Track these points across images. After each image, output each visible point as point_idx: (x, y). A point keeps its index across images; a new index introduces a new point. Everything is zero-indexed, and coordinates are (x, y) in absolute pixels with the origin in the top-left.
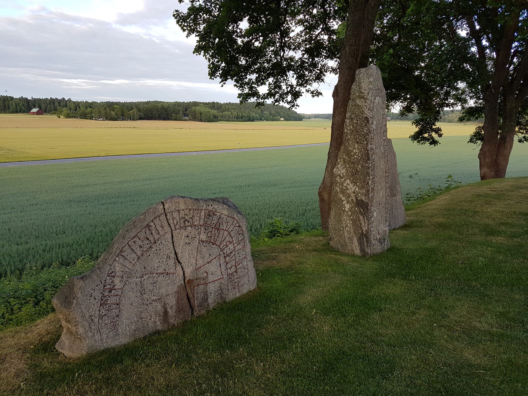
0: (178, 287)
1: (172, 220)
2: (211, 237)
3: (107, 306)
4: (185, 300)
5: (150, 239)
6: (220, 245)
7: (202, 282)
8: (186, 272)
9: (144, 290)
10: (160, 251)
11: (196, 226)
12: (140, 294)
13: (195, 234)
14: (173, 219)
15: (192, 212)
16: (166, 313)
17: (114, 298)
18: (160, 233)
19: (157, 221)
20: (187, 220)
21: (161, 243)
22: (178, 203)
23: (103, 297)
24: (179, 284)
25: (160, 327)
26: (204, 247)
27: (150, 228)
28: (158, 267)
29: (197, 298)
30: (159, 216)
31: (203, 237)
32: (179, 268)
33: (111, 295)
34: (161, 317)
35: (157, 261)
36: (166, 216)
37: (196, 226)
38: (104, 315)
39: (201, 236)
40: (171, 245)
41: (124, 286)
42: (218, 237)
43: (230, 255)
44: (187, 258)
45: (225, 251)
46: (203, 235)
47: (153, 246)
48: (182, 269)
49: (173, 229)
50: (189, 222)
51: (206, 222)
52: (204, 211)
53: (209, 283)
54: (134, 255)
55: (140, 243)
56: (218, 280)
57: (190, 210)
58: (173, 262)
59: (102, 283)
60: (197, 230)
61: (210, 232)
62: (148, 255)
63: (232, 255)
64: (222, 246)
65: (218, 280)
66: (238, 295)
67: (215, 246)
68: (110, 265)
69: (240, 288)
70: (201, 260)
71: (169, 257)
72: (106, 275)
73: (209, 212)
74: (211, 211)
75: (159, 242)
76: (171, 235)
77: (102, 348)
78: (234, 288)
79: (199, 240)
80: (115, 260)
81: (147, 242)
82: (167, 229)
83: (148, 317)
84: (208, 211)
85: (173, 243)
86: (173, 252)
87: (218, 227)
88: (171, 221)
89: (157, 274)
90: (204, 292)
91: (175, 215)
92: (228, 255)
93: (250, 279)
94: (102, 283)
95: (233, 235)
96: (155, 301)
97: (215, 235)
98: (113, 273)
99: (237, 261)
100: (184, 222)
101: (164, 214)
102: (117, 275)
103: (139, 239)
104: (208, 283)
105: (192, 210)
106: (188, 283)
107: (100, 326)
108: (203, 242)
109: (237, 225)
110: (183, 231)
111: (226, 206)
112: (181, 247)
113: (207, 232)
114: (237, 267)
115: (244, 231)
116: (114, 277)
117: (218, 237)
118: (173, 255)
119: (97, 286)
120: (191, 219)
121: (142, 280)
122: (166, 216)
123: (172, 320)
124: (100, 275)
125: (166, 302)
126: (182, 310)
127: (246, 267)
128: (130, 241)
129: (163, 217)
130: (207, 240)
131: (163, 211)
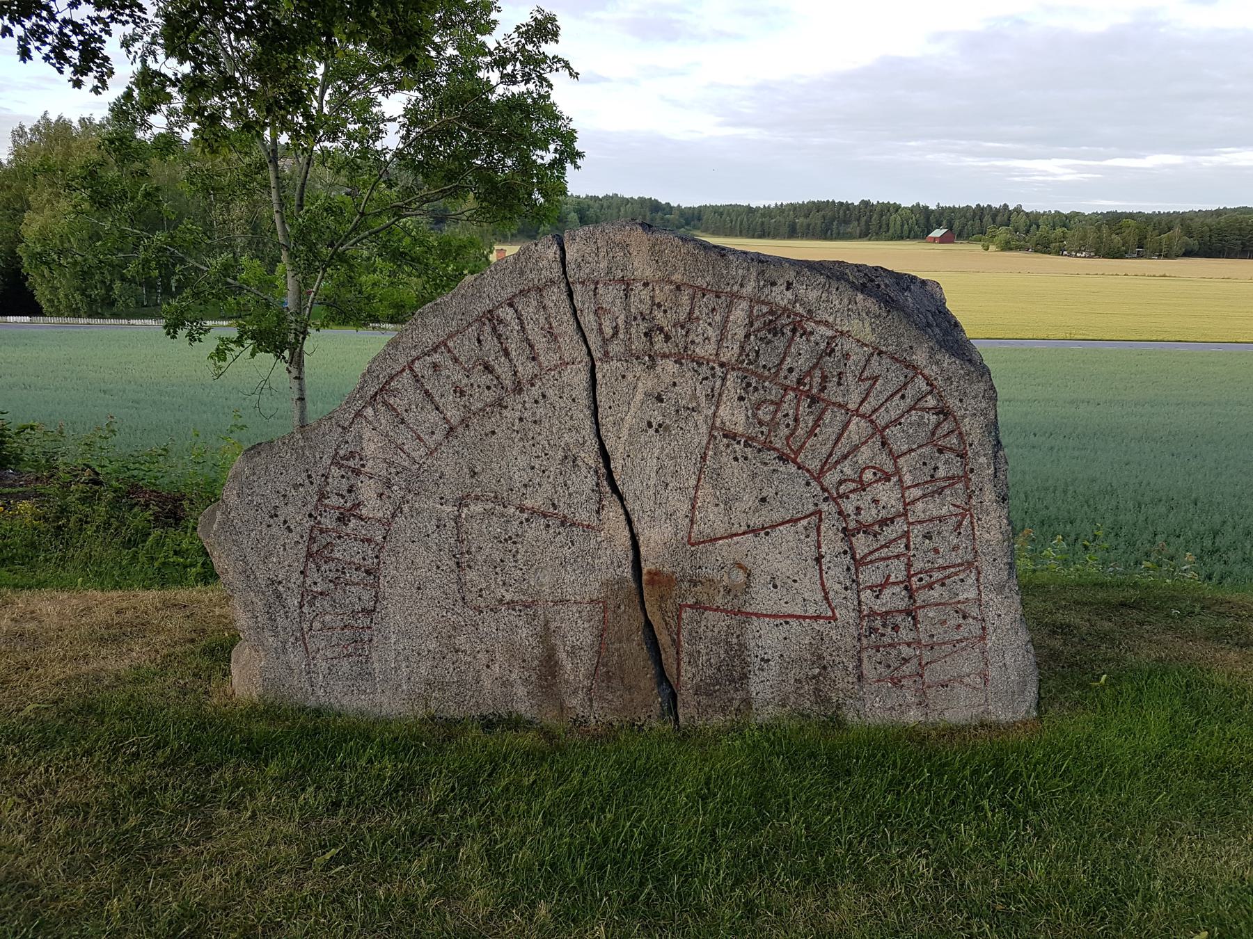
0: (606, 584)
1: (592, 317)
2: (773, 425)
3: (332, 565)
4: (635, 647)
5: (498, 370)
6: (822, 471)
7: (719, 601)
8: (642, 538)
9: (469, 552)
10: (537, 428)
11: (700, 364)
12: (452, 564)
13: (694, 396)
14: (599, 311)
15: (685, 299)
16: (549, 666)
17: (356, 546)
18: (541, 358)
19: (529, 309)
20: (661, 329)
21: (544, 396)
22: (625, 247)
23: (316, 532)
24: (609, 574)
25: (524, 707)
26: (736, 459)
27: (501, 328)
28: (525, 486)
29: (691, 655)
30: (539, 290)
31: (733, 415)
32: (613, 512)
33: (347, 535)
34: (532, 673)
35: (522, 461)
36: (570, 295)
37: (700, 364)
38: (321, 594)
39: (724, 412)
40: (582, 415)
41: (393, 516)
42: (811, 433)
43: (876, 528)
44: (651, 483)
45: (849, 508)
46: (732, 408)
47: (509, 401)
48: (629, 522)
49: (597, 354)
50: (667, 338)
51: (752, 356)
52: (744, 305)
53: (758, 615)
54: (433, 416)
55: (458, 377)
56: (805, 618)
57: (678, 288)
58: (591, 481)
59: (312, 483)
60: (706, 378)
61: (772, 402)
62: (488, 429)
63: (890, 532)
64: (831, 479)
65: (805, 618)
66: (913, 716)
67: (792, 468)
68: (343, 428)
69: (931, 693)
70: (716, 509)
71: (570, 459)
72: (327, 460)
73: (771, 312)
74: (785, 309)
75: (535, 392)
76: (585, 376)
77: (312, 703)
78: (897, 683)
79: (713, 427)
80: (359, 414)
81: (486, 379)
82: (571, 347)
83: (479, 656)
84: (765, 309)
85: (595, 413)
86: (592, 443)
87: (814, 391)
88: (588, 320)
89: (522, 511)
90: (728, 643)
91: (610, 296)
92: (865, 529)
93: (993, 672)
94: (312, 483)
95: (900, 445)
96: (511, 604)
97: (796, 420)
98: (354, 457)
99: (917, 566)
100: (646, 334)
101: (563, 286)
102: (367, 470)
103: (456, 360)
104: (748, 614)
105: (691, 291)
106: (652, 582)
107: (306, 626)
108: (731, 436)
109: (931, 402)
110: (639, 369)
111: (870, 300)
112: (624, 434)
113: (754, 397)
114: (920, 597)
115: (968, 440)
116: (357, 473)
117: (811, 433)
118: (590, 457)
119: (296, 487)
120: (683, 327)
121: (463, 516)
122: (570, 295)
123: (574, 702)
124: (307, 453)
125: (553, 625)
126: (622, 679)
127: (974, 612)
128: (418, 358)
129: (555, 295)
130: (752, 432)
131: (557, 271)
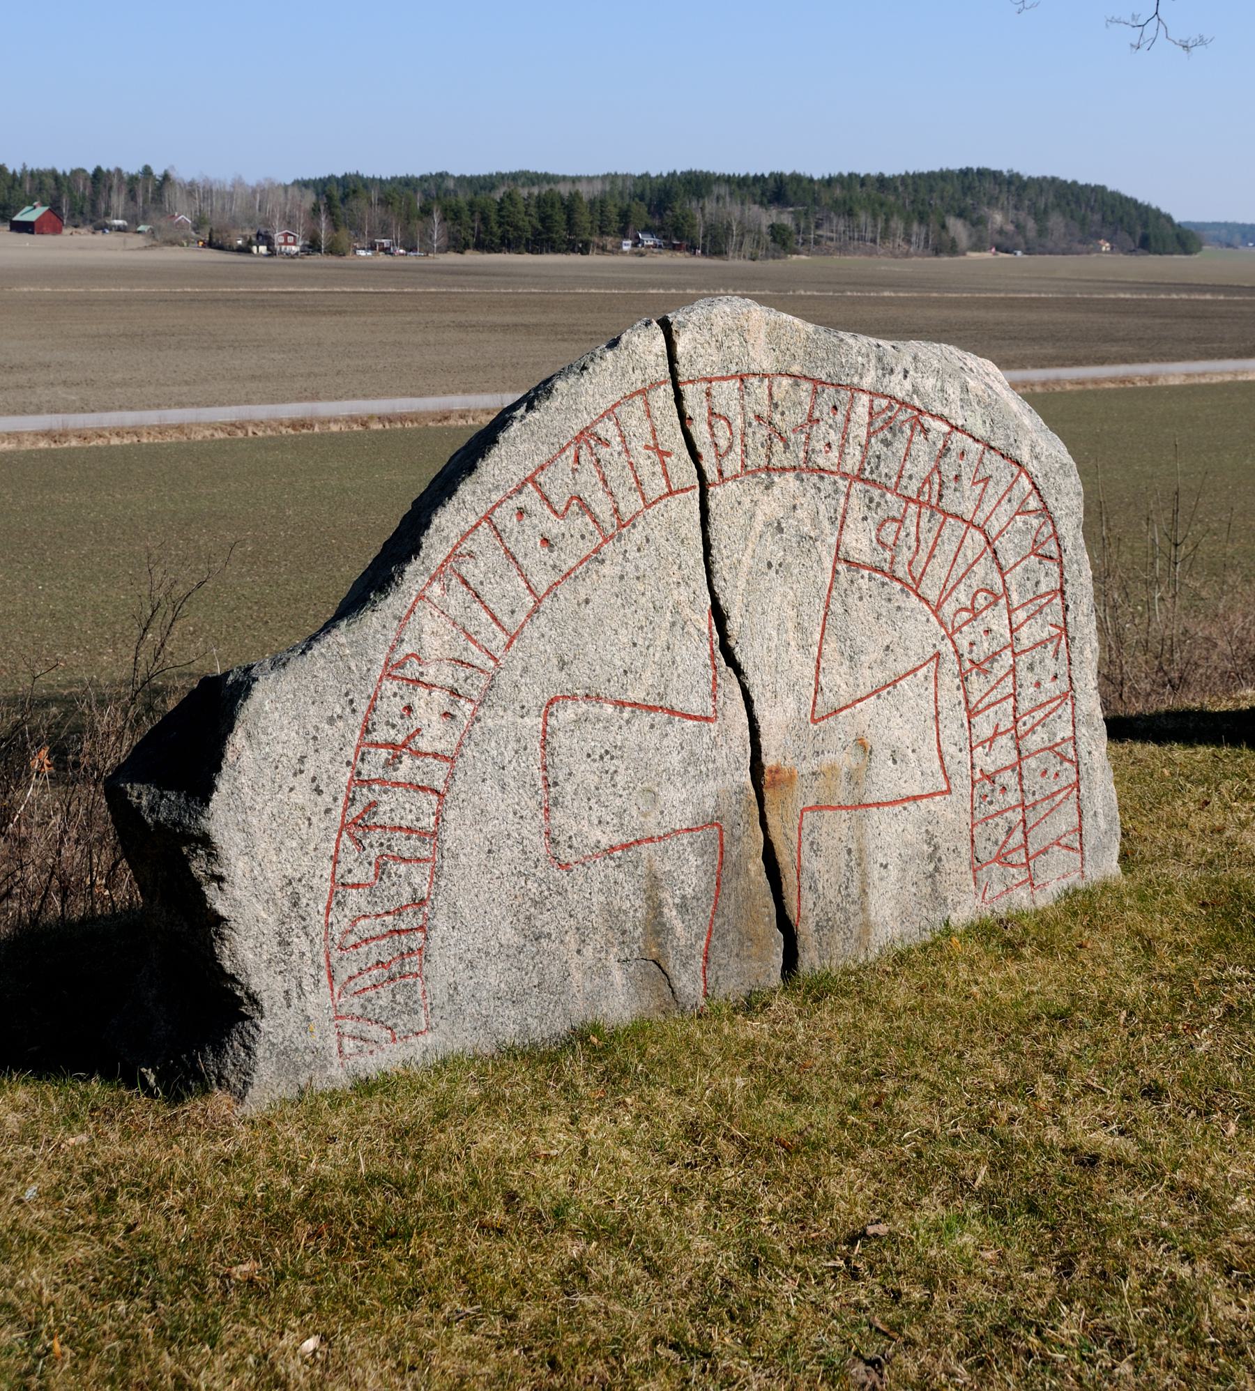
16: (657, 928)
39: (849, 538)
44: (772, 645)
49: (712, 475)
52: (865, 398)
59: (354, 711)
73: (890, 408)
79: (837, 559)
88: (700, 431)
91: (727, 392)
95: (1008, 559)
119: (331, 721)
122: (679, 398)
131: (663, 371)
